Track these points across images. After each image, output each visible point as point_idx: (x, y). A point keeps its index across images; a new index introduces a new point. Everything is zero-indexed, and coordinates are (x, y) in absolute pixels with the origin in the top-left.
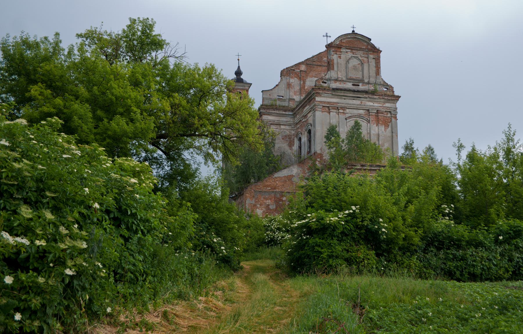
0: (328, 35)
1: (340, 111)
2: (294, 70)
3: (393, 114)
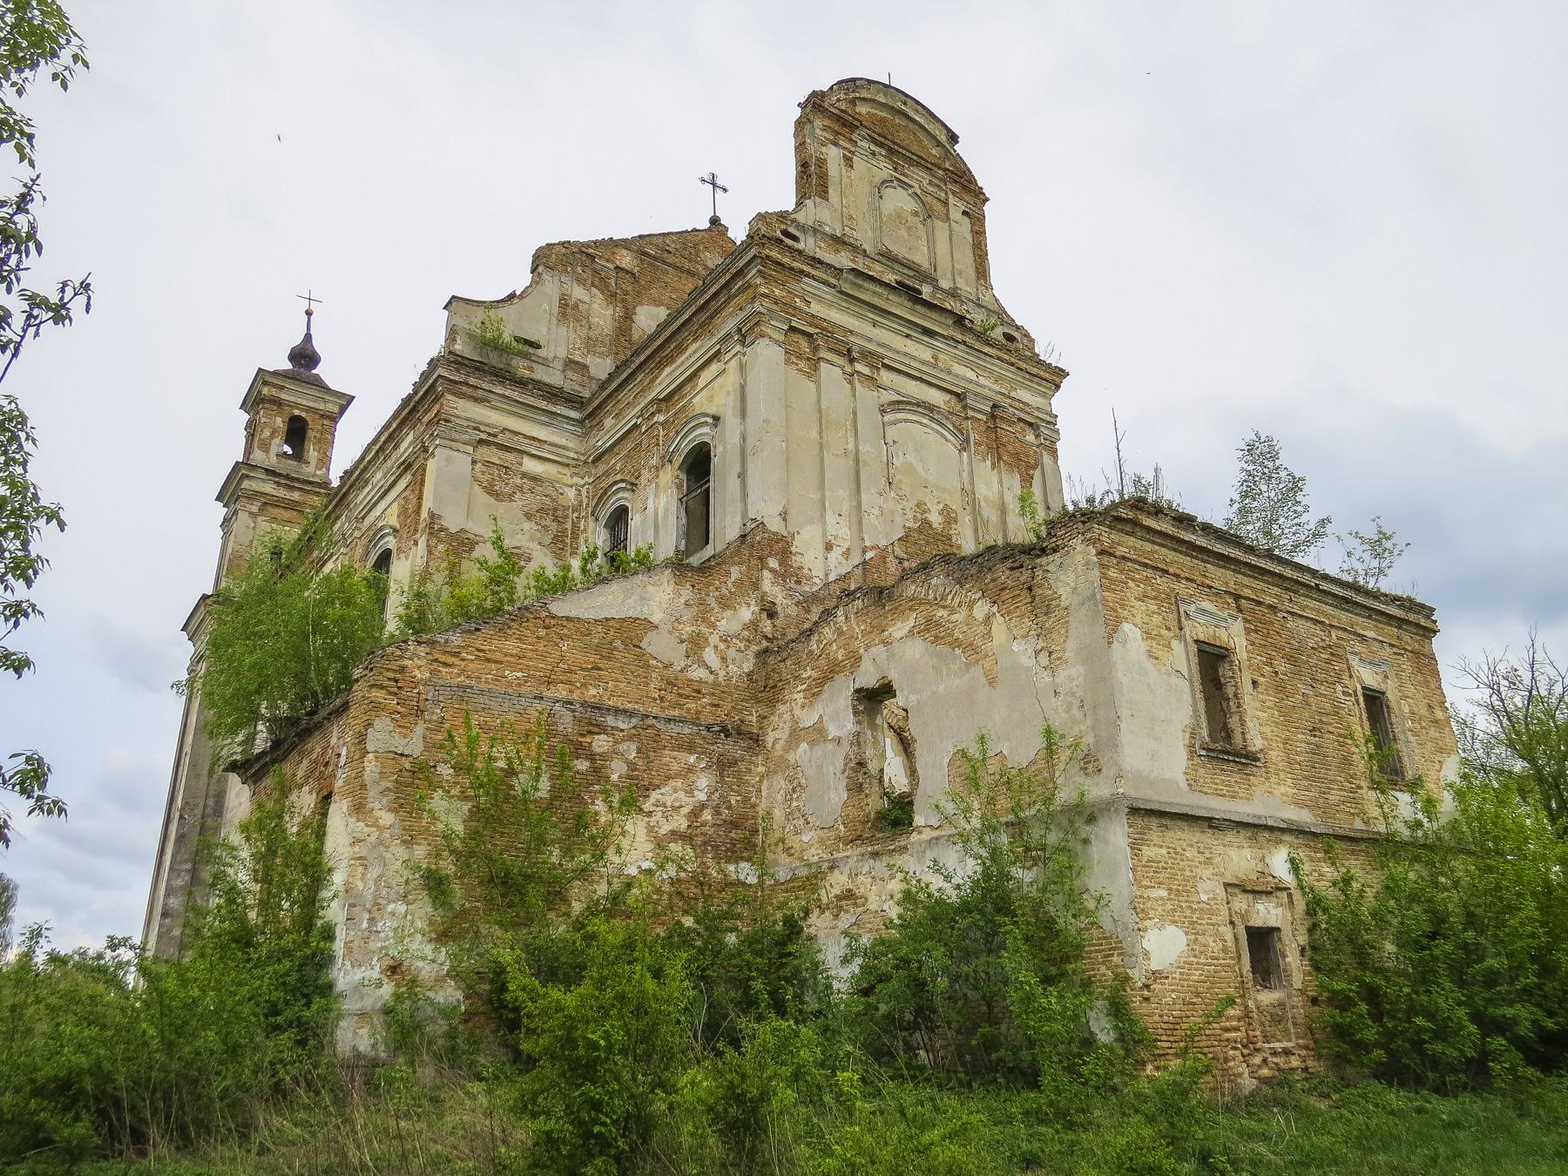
0: (719, 182)
2: (592, 257)
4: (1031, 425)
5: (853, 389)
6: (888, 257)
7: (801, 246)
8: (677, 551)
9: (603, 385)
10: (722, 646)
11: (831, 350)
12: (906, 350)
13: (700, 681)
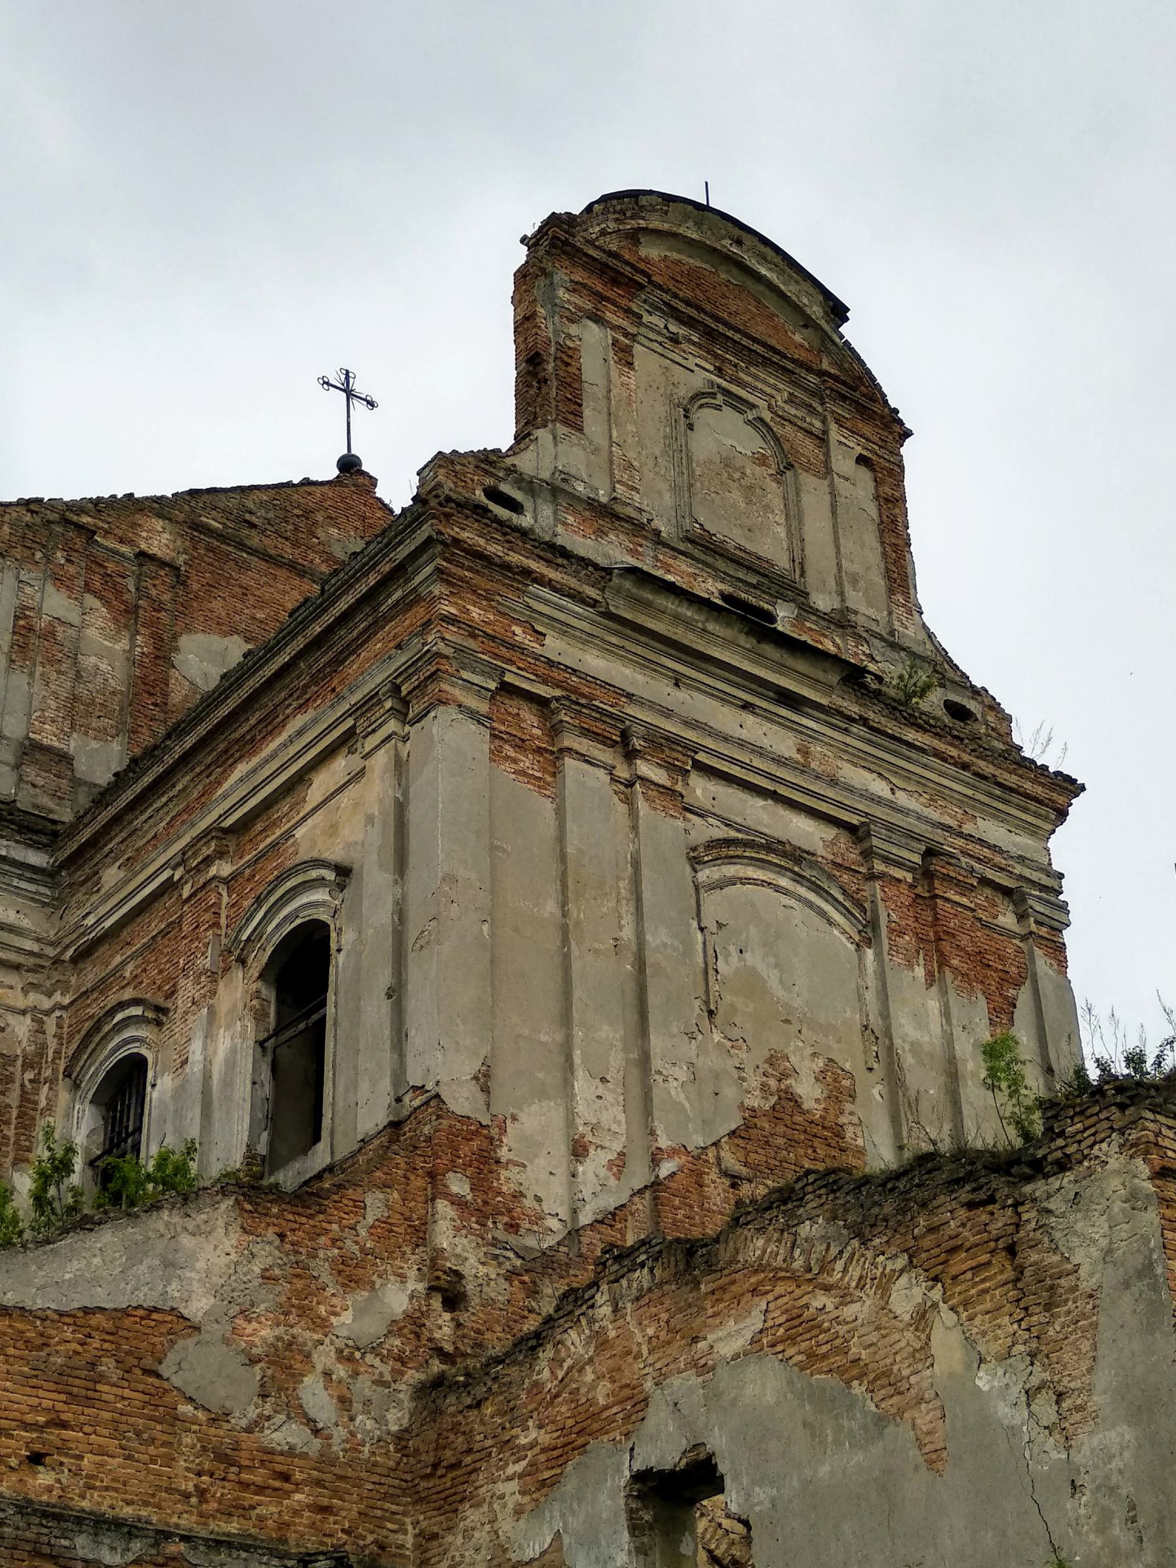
0: (358, 386)
1: (644, 768)
2: (89, 533)
3: (1038, 905)
4: (1007, 892)
5: (633, 813)
6: (705, 547)
7: (525, 520)
8: (251, 1156)
9: (103, 797)
10: (341, 1371)
11: (586, 733)
12: (744, 734)
13: (291, 1452)
